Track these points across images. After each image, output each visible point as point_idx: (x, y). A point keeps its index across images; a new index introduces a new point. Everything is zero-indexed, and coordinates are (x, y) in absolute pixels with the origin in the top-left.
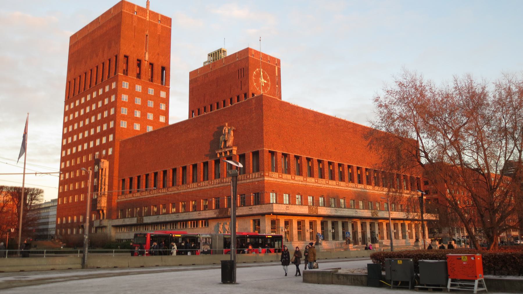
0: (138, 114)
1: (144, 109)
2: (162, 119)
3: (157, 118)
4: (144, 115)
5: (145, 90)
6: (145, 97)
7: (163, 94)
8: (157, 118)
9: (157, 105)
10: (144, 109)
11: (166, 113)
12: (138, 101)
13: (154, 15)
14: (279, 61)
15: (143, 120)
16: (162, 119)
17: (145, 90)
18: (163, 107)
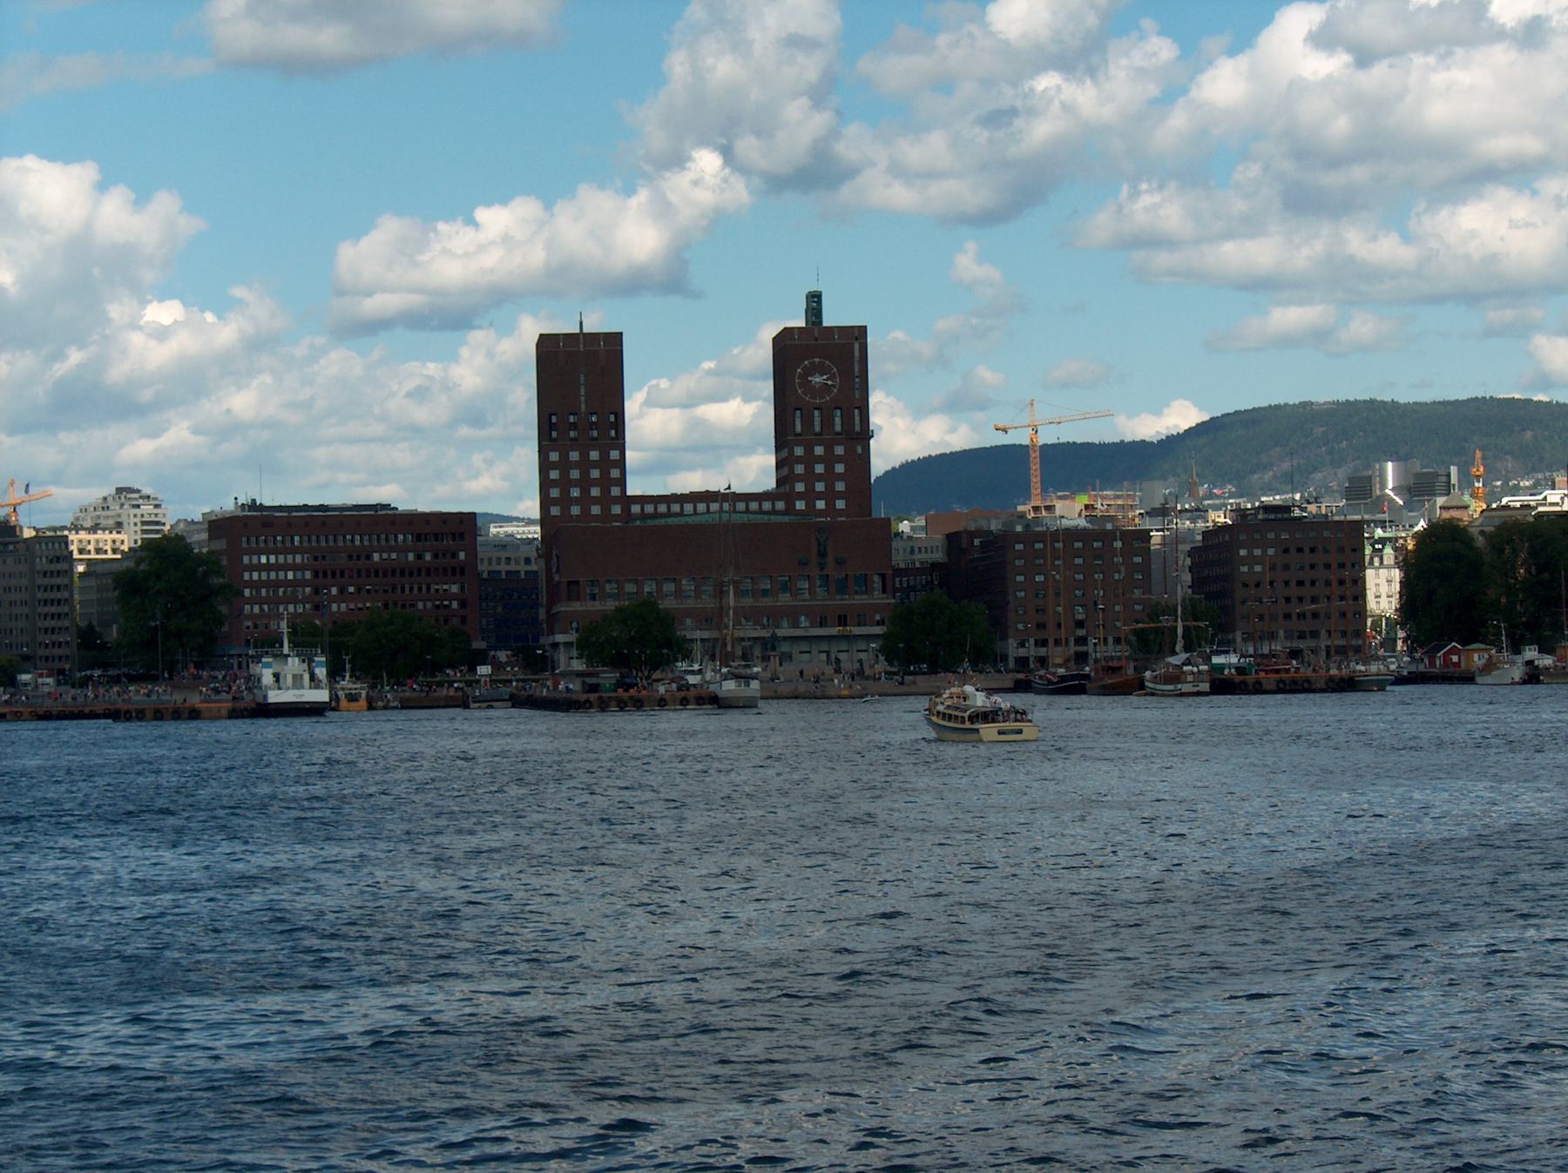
0: (575, 493)
1: (585, 484)
2: (615, 491)
3: (606, 491)
4: (585, 491)
5: (584, 456)
6: (585, 465)
7: (614, 455)
8: (606, 491)
9: (605, 474)
10: (585, 484)
11: (622, 482)
12: (575, 474)
13: (594, 337)
14: (863, 330)
15: (585, 500)
16: (615, 491)
17: (584, 456)
18: (615, 473)
